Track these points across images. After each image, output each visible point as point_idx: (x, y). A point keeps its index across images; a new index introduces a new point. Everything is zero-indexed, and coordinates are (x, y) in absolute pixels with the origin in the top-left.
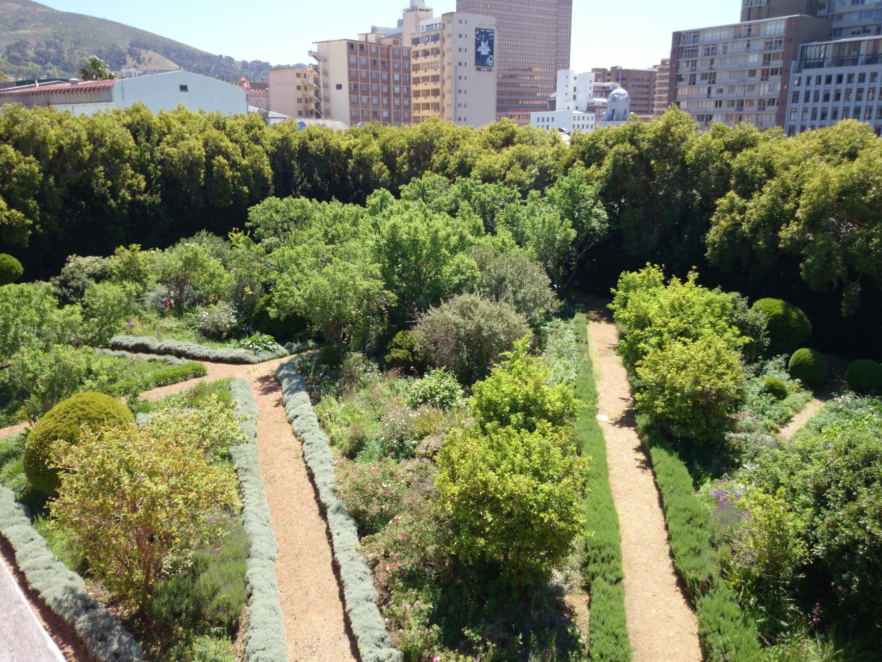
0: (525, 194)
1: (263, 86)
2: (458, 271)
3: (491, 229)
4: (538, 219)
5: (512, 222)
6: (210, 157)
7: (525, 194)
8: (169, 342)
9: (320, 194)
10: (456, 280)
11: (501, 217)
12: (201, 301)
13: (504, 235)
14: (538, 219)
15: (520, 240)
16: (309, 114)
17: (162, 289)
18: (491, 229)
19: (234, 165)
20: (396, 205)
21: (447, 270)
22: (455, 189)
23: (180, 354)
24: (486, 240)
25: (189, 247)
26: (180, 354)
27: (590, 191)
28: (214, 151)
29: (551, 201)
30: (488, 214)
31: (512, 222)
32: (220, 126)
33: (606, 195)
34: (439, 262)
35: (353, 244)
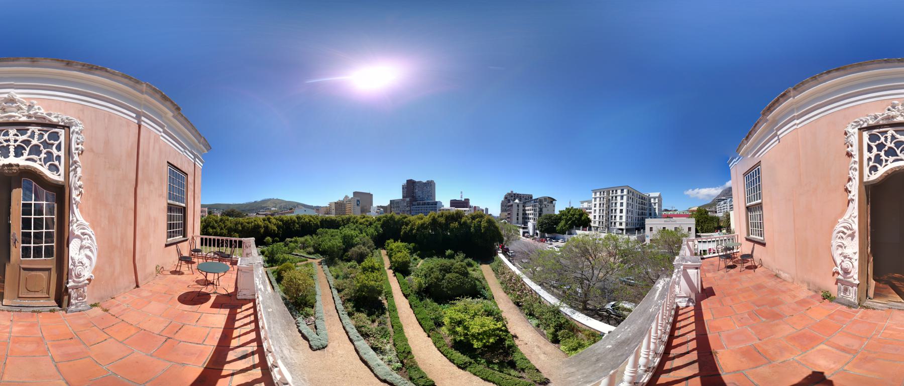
0: (367, 227)
1: (318, 210)
2: (356, 241)
3: (362, 233)
4: (370, 231)
5: (366, 232)
6: (309, 222)
7: (367, 227)
8: (302, 254)
9: (329, 228)
10: (356, 243)
11: (363, 231)
12: (308, 247)
13: (364, 234)
14: (370, 231)
15: (367, 235)
16: (326, 214)
17: (301, 244)
18: (362, 233)
19: (313, 223)
20: (344, 229)
21: (354, 241)
22: (355, 226)
23: (303, 257)
24: (361, 235)
25: (306, 237)
26: (303, 257)
27: (379, 226)
28: (310, 221)
29: (372, 228)
30: (361, 230)
31: (366, 232)
32: (311, 217)
33: (382, 226)
34: (353, 239)
35: (337, 237)
